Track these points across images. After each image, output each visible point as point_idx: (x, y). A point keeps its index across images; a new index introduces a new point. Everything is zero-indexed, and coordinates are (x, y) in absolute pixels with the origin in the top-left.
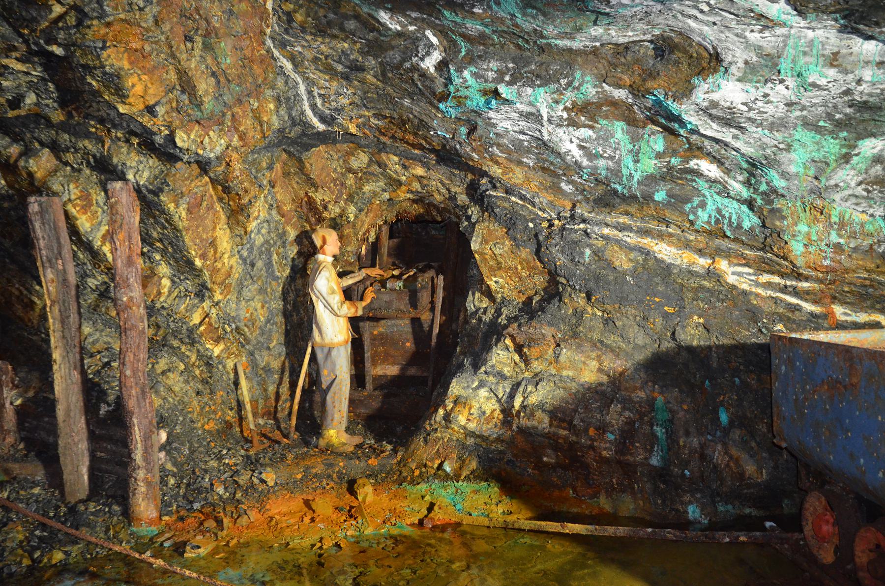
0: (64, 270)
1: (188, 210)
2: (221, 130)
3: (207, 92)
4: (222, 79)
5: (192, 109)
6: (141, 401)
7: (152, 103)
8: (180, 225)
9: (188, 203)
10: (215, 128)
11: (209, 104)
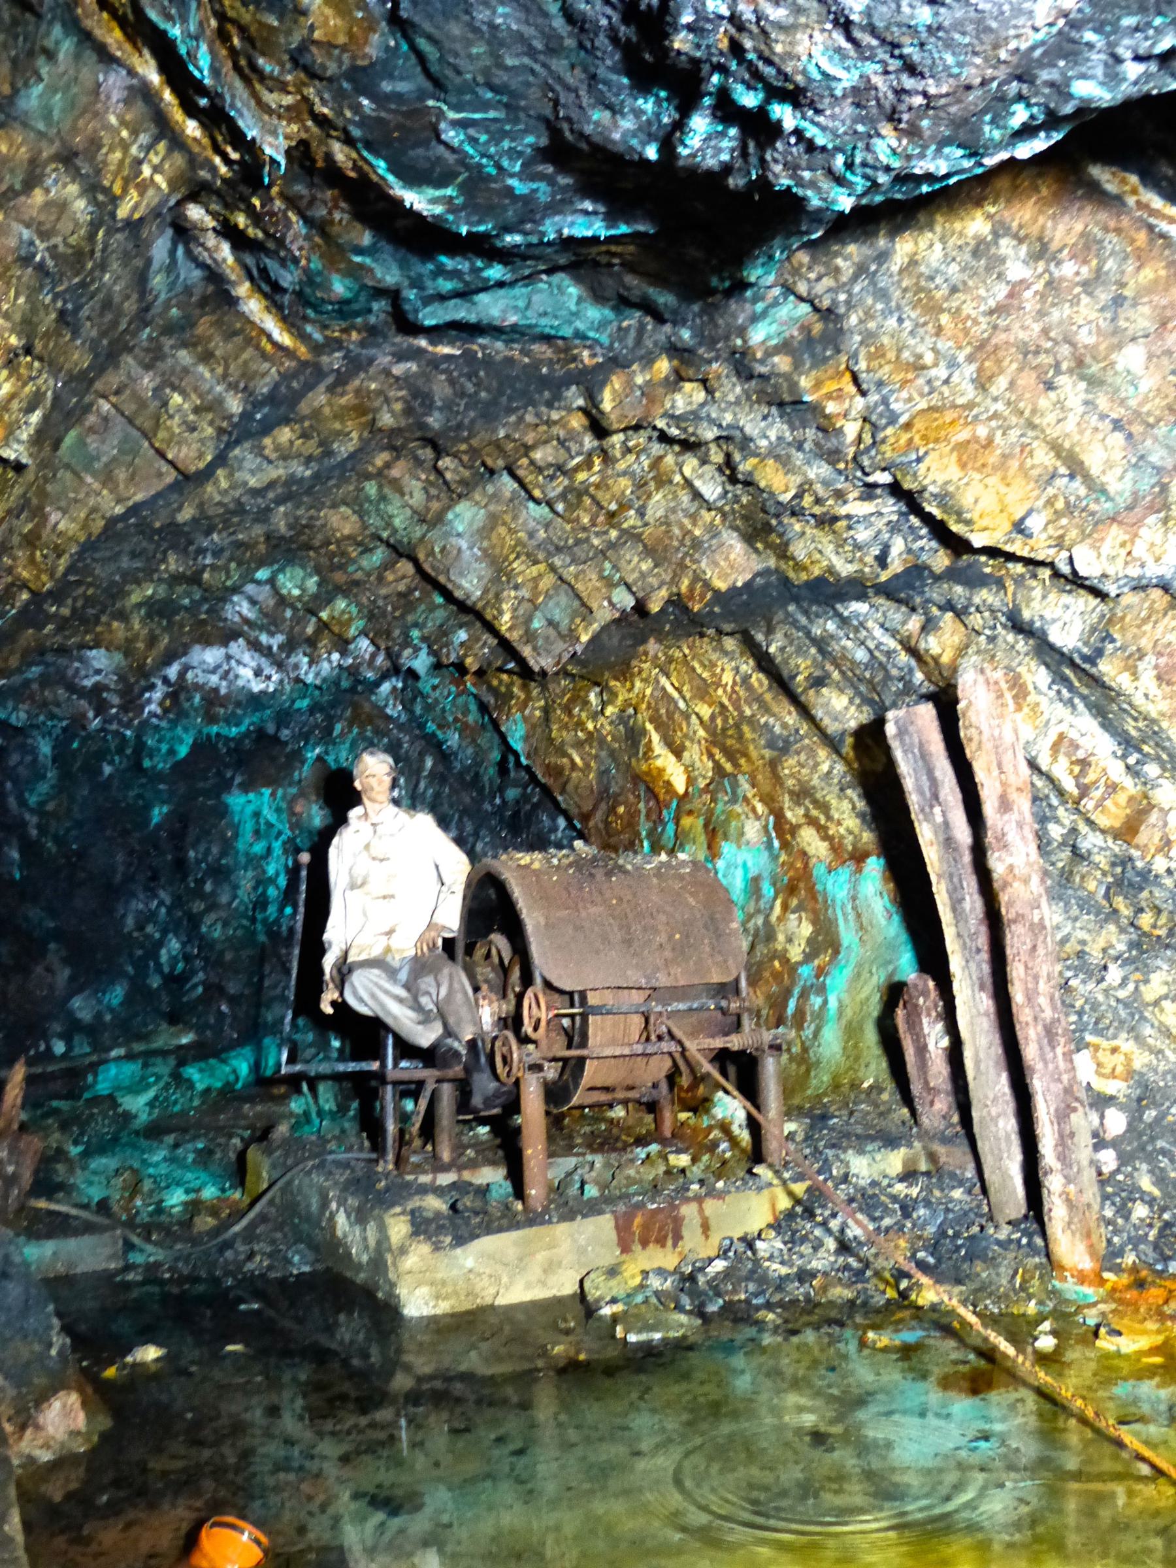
0: (946, 824)
1: (1159, 678)
2: (1165, 521)
3: (1109, 465)
4: (1137, 429)
5: (1097, 501)
6: (1047, 1049)
7: (1018, 516)
8: (1153, 711)
9: (1156, 667)
10: (1152, 519)
11: (1120, 485)
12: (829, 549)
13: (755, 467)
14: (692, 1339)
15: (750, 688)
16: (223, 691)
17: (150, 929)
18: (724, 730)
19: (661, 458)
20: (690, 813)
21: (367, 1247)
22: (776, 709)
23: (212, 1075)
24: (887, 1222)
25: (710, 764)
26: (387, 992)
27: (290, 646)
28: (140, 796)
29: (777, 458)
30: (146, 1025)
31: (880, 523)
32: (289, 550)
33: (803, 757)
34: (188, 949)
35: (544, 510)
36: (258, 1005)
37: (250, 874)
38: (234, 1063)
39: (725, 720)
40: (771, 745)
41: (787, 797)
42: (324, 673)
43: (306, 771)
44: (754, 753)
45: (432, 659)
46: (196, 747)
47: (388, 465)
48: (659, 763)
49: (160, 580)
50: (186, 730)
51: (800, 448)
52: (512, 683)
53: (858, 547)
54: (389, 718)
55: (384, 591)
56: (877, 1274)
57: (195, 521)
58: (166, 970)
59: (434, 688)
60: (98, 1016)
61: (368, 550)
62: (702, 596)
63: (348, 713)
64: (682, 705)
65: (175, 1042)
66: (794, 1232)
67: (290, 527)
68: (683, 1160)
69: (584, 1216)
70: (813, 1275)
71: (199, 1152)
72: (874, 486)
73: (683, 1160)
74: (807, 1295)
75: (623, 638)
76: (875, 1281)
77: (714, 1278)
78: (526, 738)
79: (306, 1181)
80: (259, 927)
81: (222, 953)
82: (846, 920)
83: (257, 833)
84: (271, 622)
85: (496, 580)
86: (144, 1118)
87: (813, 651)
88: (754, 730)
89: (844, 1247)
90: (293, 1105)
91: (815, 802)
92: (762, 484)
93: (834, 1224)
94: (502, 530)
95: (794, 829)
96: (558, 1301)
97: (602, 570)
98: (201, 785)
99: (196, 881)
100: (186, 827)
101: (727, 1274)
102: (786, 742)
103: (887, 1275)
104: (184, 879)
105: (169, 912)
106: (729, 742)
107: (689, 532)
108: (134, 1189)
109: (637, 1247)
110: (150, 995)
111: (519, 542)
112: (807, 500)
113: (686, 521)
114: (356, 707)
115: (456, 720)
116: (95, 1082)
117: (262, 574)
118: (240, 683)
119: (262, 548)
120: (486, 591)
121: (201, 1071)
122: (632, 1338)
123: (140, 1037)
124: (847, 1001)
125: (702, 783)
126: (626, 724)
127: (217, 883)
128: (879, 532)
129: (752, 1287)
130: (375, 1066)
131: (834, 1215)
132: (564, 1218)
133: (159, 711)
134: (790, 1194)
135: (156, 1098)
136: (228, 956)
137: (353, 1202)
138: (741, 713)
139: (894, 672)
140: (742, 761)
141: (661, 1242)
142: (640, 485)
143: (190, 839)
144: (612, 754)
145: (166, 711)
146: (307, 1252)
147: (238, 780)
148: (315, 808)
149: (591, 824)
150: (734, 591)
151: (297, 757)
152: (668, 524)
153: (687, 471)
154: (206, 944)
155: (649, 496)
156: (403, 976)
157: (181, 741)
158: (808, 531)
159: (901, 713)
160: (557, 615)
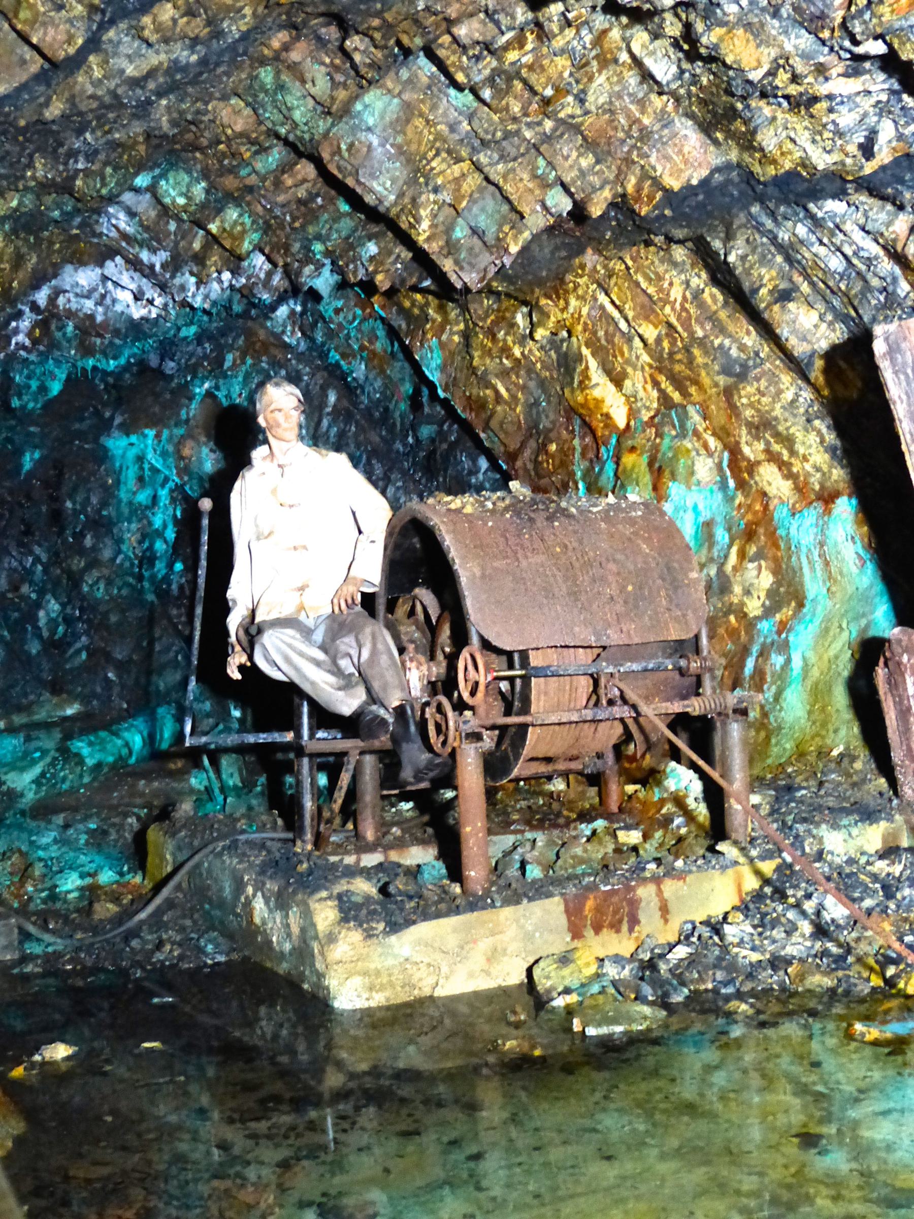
12: (804, 138)
13: (721, 39)
14: (655, 1034)
15: (701, 305)
16: (99, 318)
17: (25, 589)
18: (671, 354)
19: (605, 32)
20: (633, 449)
21: (289, 935)
22: (731, 328)
23: (103, 750)
24: (868, 903)
25: (655, 394)
26: (302, 654)
27: (175, 265)
29: (748, 26)
30: (26, 695)
31: (867, 104)
32: (172, 152)
33: (763, 383)
34: (69, 610)
35: (467, 98)
36: (149, 673)
37: (134, 526)
38: (126, 735)
39: (673, 343)
40: (726, 371)
41: (744, 431)
42: (213, 296)
43: (194, 409)
44: (706, 380)
45: (337, 277)
46: (69, 382)
47: (286, 48)
48: (596, 393)
49: (26, 189)
50: (58, 363)
51: (776, 14)
52: (427, 304)
53: (839, 134)
54: (287, 347)
55: (281, 199)
56: (859, 960)
57: (65, 117)
58: (45, 634)
59: (337, 311)
61: (263, 150)
62: (651, 198)
63: (241, 341)
64: (623, 325)
65: (60, 713)
66: (764, 915)
67: (174, 123)
68: (633, 837)
69: (530, 899)
70: (788, 962)
71: (91, 833)
72: (865, 57)
73: (633, 837)
74: (782, 984)
75: (557, 248)
76: (857, 968)
77: (677, 966)
78: (443, 368)
79: (218, 863)
80: (146, 584)
81: (106, 615)
82: (813, 569)
83: (141, 479)
84: (154, 239)
85: (412, 181)
86: (30, 796)
87: (779, 259)
88: (706, 353)
89: (821, 931)
90: (193, 781)
91: (777, 435)
92: (729, 61)
93: (809, 906)
94: (419, 122)
95: (752, 467)
96: (504, 992)
97: (535, 168)
98: (77, 426)
99: (74, 535)
100: (61, 475)
101: (692, 961)
102: (745, 367)
103: (871, 961)
105: (45, 571)
106: (678, 368)
107: (638, 121)
108: (25, 873)
109: (589, 933)
110: (28, 661)
111: (439, 137)
112: (783, 77)
113: (633, 108)
114: (249, 334)
115: (362, 348)
117: (142, 181)
118: (119, 308)
119: (142, 149)
120: (401, 195)
121: (91, 744)
122: (591, 1031)
123: (20, 709)
124: (812, 657)
125: (645, 416)
126: (558, 349)
127: (97, 537)
128: (865, 115)
129: (720, 975)
130: (289, 736)
131: (809, 896)
132: (507, 902)
133: (27, 342)
134: (758, 873)
135: (43, 775)
136: (113, 618)
137: (272, 886)
138: (692, 333)
139: (875, 282)
140: (693, 390)
141: (616, 927)
142: (581, 66)
143: (65, 489)
144: (542, 384)
145: (35, 342)
146: (221, 940)
147: (118, 420)
148: (205, 450)
149: (519, 464)
150: (689, 191)
151: (184, 392)
152: (612, 112)
153: (636, 48)
154: (89, 607)
155: (591, 79)
156: (319, 636)
157: (53, 377)
158: (779, 115)
159: (892, 327)
160: (482, 222)
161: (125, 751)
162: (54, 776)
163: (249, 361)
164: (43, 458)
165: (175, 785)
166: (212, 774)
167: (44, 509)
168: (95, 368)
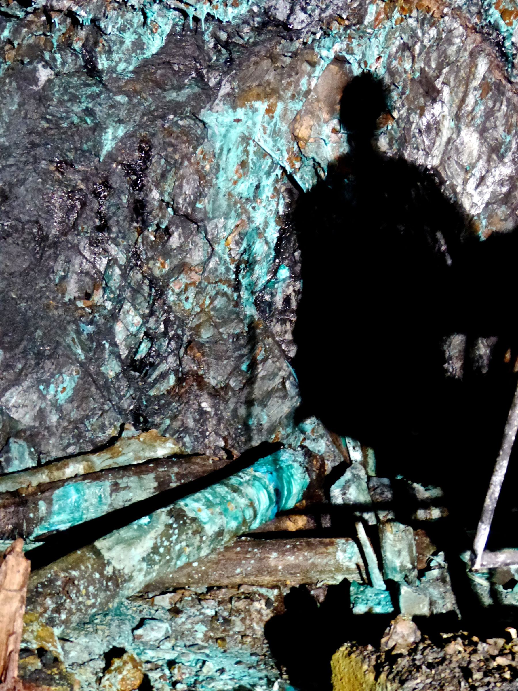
17: (98, 297)
23: (225, 512)
28: (89, 112)
36: (249, 403)
37: (232, 223)
38: (250, 491)
60: (41, 415)
65: (150, 454)
80: (245, 294)
81: (197, 329)
83: (243, 164)
90: (340, 555)
98: (173, 95)
100: (147, 158)
104: (145, 225)
105: (124, 276)
116: (50, 513)
121: (209, 505)
123: (99, 449)
127: (187, 236)
135: (155, 550)
136: (206, 334)
143: (152, 175)
147: (225, 89)
148: (326, 130)
161: (249, 513)
162: (168, 550)
163: (396, 15)
164: (129, 136)
165: (319, 560)
166: (369, 550)
167: (124, 199)
168: (210, 17)
